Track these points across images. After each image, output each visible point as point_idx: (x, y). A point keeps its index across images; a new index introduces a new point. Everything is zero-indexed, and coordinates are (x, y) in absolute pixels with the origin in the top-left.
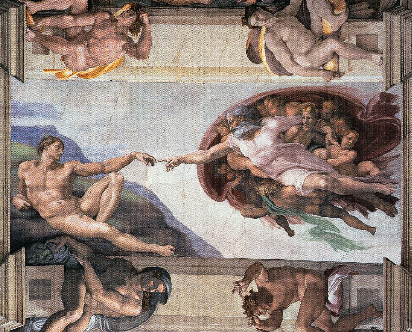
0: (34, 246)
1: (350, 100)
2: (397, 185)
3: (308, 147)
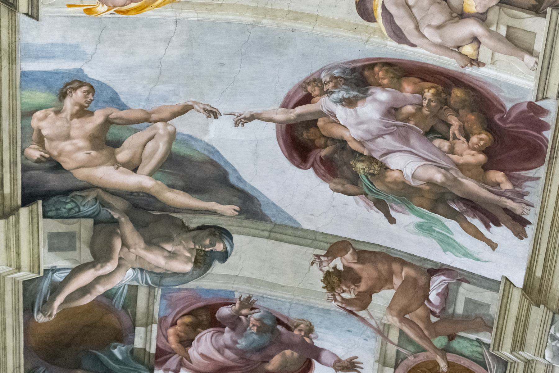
0: (55, 198)
1: (489, 97)
2: (531, 208)
3: (427, 134)
